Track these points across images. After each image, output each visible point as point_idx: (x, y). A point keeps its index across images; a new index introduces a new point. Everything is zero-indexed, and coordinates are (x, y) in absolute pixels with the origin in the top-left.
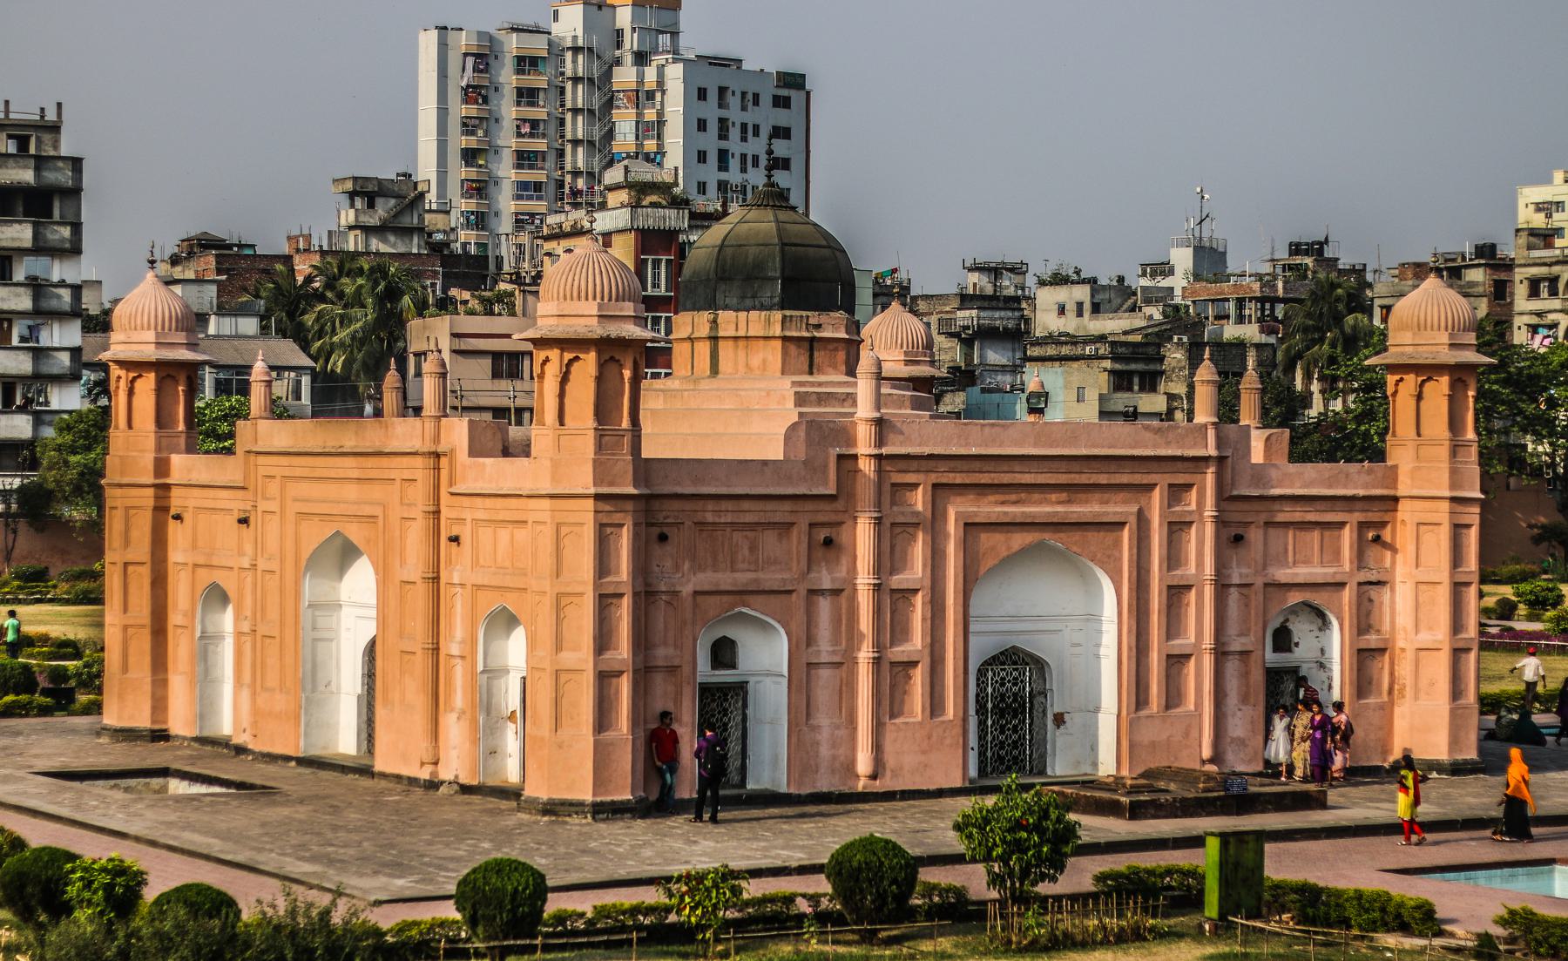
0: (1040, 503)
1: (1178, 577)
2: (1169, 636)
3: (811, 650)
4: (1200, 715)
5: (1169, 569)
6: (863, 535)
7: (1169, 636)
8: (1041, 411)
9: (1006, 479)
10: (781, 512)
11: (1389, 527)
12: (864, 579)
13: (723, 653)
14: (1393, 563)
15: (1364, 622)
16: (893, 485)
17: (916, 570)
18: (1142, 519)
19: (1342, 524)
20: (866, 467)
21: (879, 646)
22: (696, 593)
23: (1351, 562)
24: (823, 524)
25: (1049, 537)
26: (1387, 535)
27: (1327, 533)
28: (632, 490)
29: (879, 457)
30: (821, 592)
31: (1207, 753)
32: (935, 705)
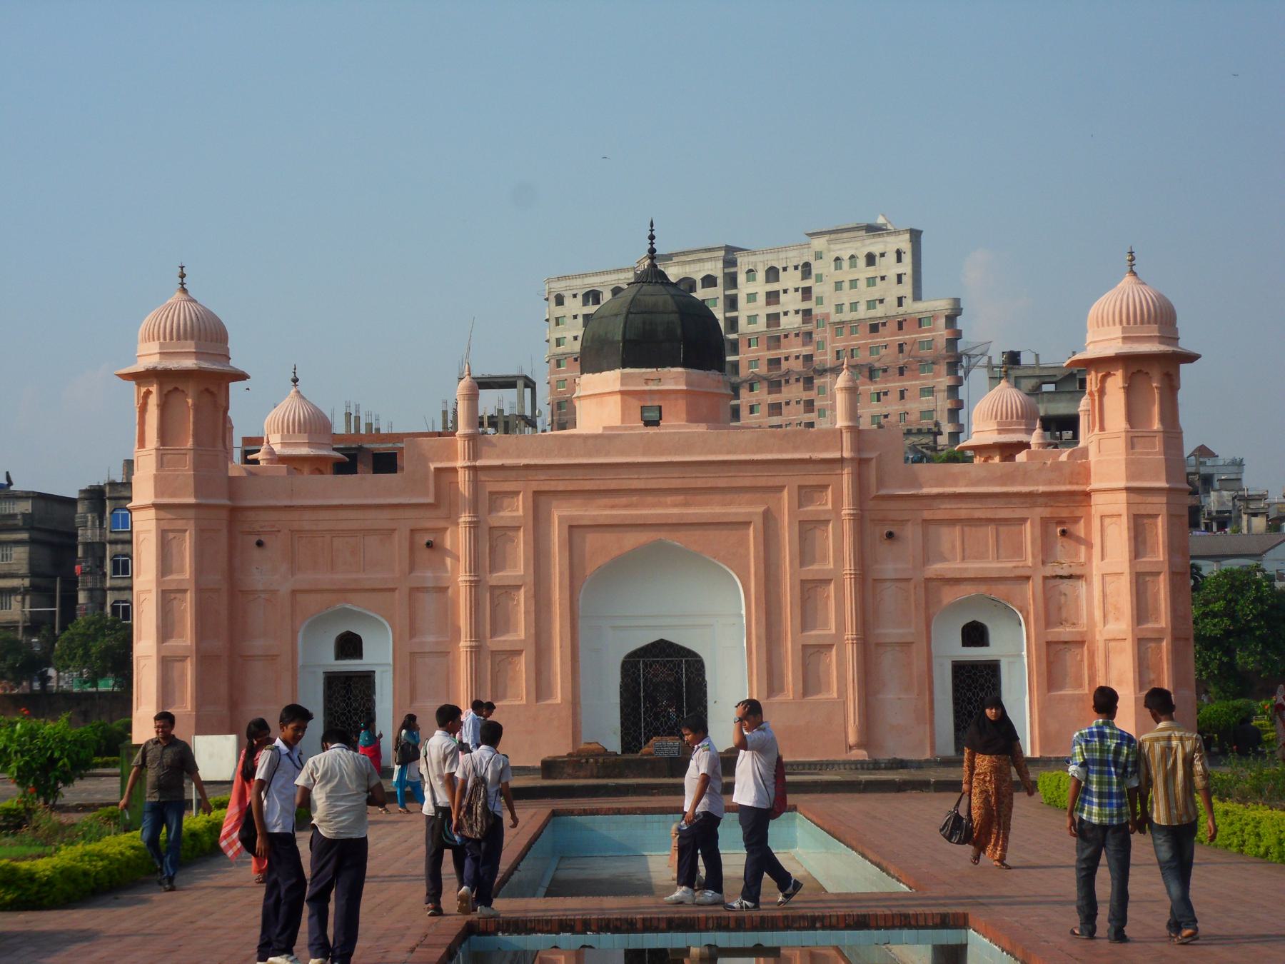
0: (654, 506)
2: (804, 627)
3: (415, 640)
4: (845, 703)
5: (802, 563)
6: (458, 538)
7: (804, 627)
8: (655, 423)
9: (613, 485)
11: (1082, 521)
12: (463, 577)
13: (349, 645)
15: (1052, 612)
16: (491, 493)
17: (517, 567)
18: (769, 518)
19: (1024, 520)
20: (463, 479)
21: (476, 633)
22: (294, 592)
24: (426, 530)
25: (663, 535)
26: (1080, 529)
27: (1002, 529)
29: (474, 469)
31: (852, 739)
32: (541, 688)
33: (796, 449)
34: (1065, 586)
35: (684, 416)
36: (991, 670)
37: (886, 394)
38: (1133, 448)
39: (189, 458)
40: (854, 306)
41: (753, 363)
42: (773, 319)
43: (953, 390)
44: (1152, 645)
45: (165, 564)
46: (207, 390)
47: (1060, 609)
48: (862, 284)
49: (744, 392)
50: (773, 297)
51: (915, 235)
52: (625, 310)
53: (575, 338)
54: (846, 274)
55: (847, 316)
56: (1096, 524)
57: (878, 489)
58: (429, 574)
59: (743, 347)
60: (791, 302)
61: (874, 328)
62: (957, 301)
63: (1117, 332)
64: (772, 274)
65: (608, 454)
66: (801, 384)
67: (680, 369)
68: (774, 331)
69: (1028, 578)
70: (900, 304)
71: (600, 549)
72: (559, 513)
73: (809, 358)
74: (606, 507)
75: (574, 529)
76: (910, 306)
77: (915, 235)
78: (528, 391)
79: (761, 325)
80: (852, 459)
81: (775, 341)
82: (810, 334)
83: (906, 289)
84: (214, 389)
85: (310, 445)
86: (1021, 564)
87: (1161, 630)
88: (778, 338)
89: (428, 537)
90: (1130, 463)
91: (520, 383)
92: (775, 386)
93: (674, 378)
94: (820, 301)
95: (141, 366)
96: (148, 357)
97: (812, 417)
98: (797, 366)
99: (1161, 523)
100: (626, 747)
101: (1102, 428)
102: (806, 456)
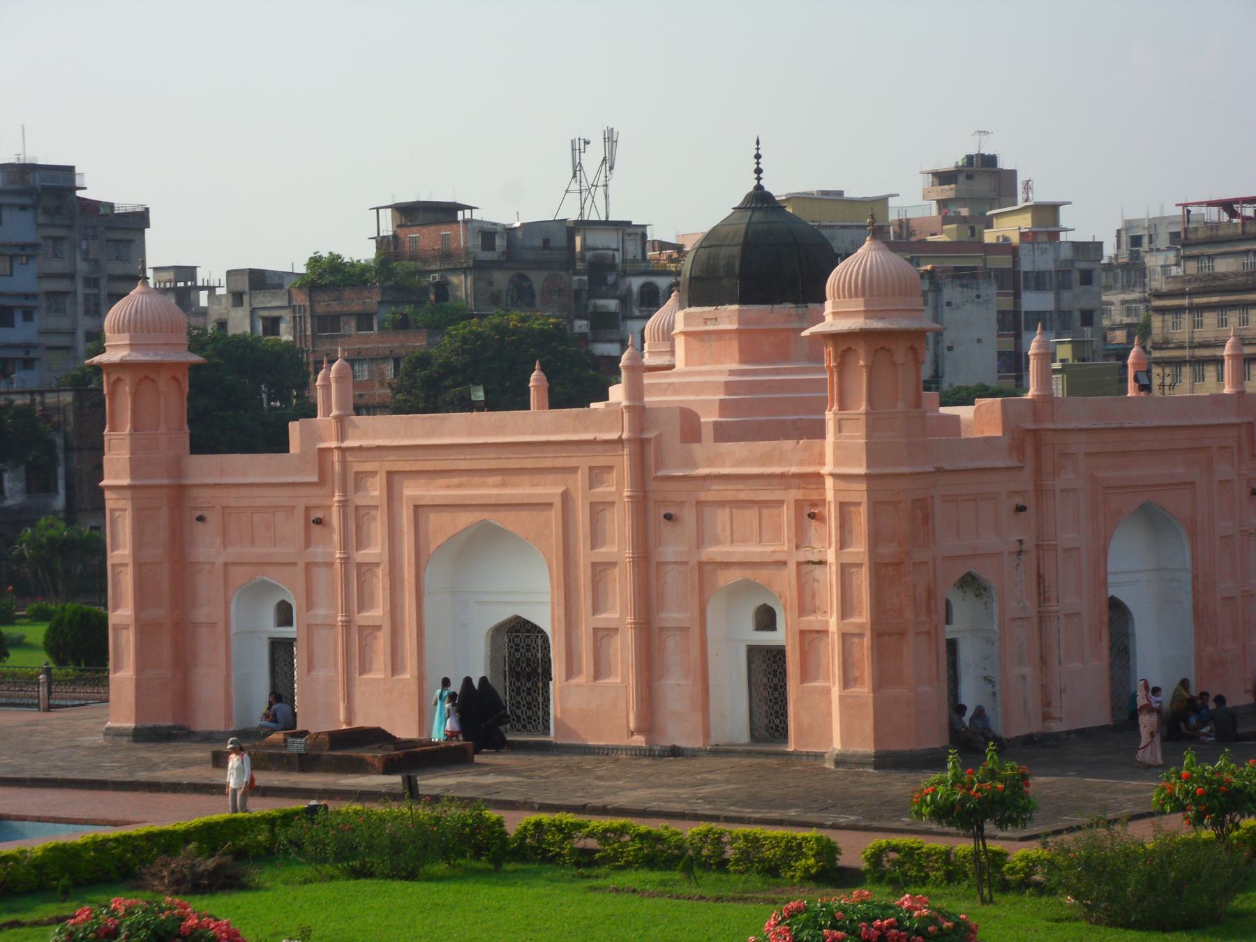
0: (479, 486)
2: (595, 611)
3: (311, 613)
10: (283, 497)
16: (357, 473)
19: (780, 503)
27: (766, 512)
28: (164, 481)
30: (316, 564)
31: (632, 725)
35: (737, 357)
38: (840, 431)
44: (856, 640)
46: (146, 377)
47: (814, 595)
57: (657, 469)
58: (320, 550)
65: (441, 435)
67: (736, 307)
69: (785, 563)
72: (412, 491)
80: (629, 440)
86: (779, 548)
87: (862, 625)
102: (590, 436)
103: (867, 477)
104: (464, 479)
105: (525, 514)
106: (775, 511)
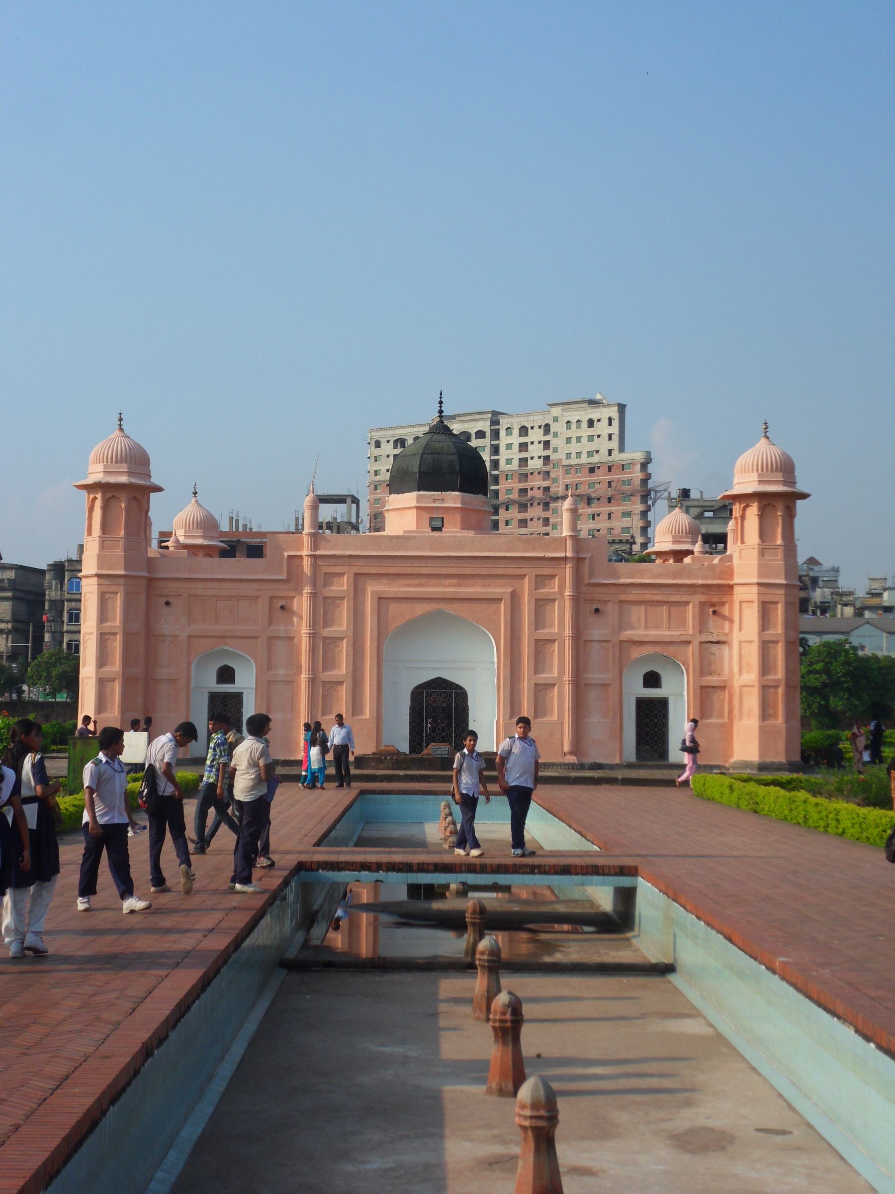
0: (436, 585)
1: (544, 633)
2: (536, 672)
4: (562, 724)
6: (302, 604)
7: (536, 672)
8: (440, 529)
9: (409, 571)
11: (727, 605)
12: (304, 630)
13: (226, 675)
14: (731, 630)
15: (705, 666)
17: (342, 625)
18: (515, 597)
19: (688, 603)
20: (307, 564)
21: (313, 669)
22: (190, 637)
23: (694, 628)
24: (281, 597)
26: (726, 610)
27: (674, 609)
30: (277, 638)
31: (566, 748)
33: (534, 550)
34: (714, 648)
36: (662, 705)
37: (598, 515)
39: (121, 544)
40: (578, 455)
41: (509, 491)
42: (523, 462)
43: (644, 514)
44: (772, 690)
45: (103, 615)
47: (710, 664)
48: (584, 440)
49: (502, 511)
50: (523, 447)
51: (622, 408)
52: (421, 452)
53: (388, 471)
54: (574, 433)
55: (574, 461)
56: (736, 607)
57: (590, 579)
58: (281, 628)
59: (502, 480)
60: (536, 450)
61: (592, 470)
62: (649, 453)
63: (755, 477)
64: (524, 431)
65: (406, 549)
66: (541, 506)
67: (457, 493)
68: (524, 470)
69: (689, 642)
70: (610, 454)
71: (399, 614)
72: (372, 589)
73: (547, 489)
74: (403, 586)
75: (382, 600)
76: (616, 456)
77: (622, 408)
78: (354, 505)
79: (515, 465)
80: (572, 558)
81: (524, 477)
82: (548, 473)
83: (614, 444)
84: (139, 496)
85: (204, 537)
86: (685, 633)
87: (778, 680)
88: (526, 475)
89: (281, 603)
90: (760, 566)
91: (349, 500)
92: (523, 507)
93: (453, 499)
94: (555, 450)
95: (90, 480)
96: (96, 474)
97: (548, 529)
98: (539, 494)
99: (780, 609)
100: (412, 750)
101: (742, 542)
102: (542, 555)
103: (786, 586)
104: (423, 581)
105: (476, 606)
106: (681, 608)
